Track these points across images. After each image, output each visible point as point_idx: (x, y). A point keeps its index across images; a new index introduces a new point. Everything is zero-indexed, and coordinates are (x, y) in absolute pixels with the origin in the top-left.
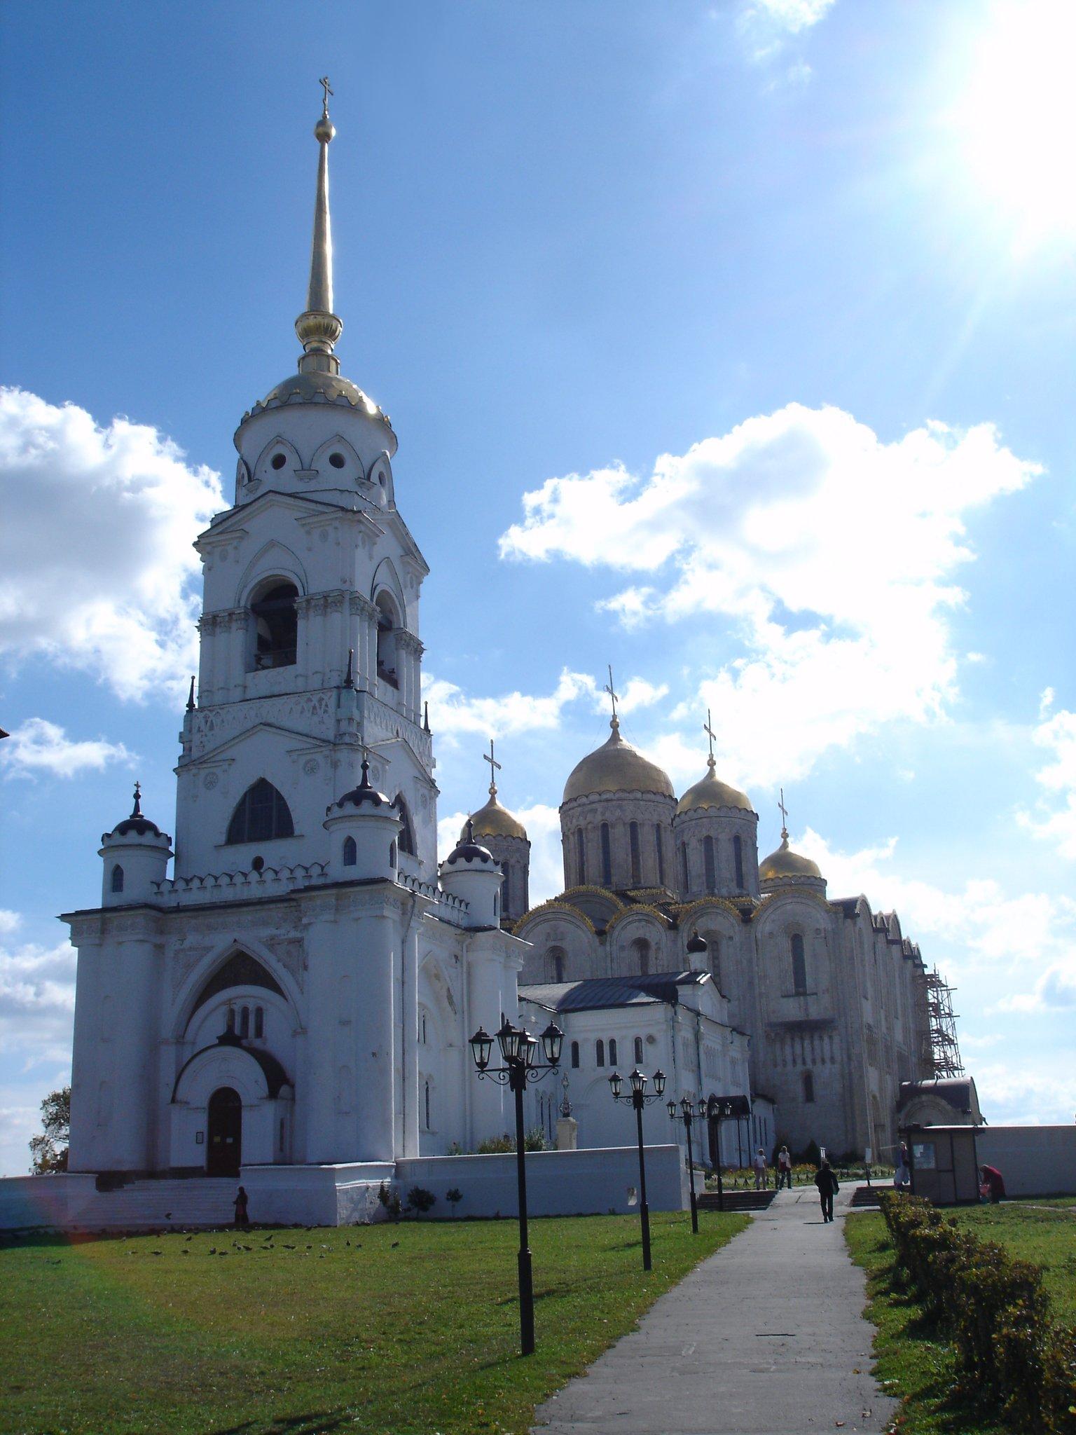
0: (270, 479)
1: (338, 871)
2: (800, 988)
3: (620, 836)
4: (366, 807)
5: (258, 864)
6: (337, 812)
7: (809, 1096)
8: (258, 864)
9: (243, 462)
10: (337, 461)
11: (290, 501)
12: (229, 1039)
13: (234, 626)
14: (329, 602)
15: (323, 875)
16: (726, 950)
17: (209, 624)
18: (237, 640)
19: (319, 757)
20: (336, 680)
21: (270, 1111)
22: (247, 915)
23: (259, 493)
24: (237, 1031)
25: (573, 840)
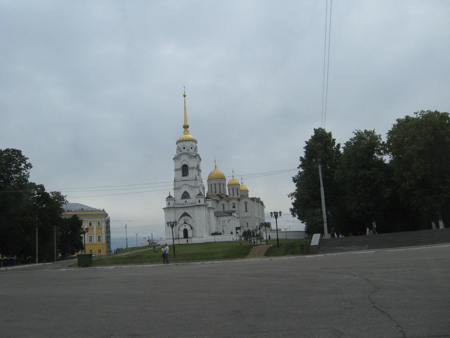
0: (183, 151)
1: (198, 204)
2: (246, 211)
3: (218, 186)
4: (201, 196)
5: (186, 201)
7: (248, 226)
8: (186, 201)
9: (178, 147)
10: (192, 148)
12: (185, 223)
14: (193, 168)
16: (236, 206)
17: (176, 170)
18: (180, 173)
21: (191, 231)
22: (186, 209)
25: (210, 186)
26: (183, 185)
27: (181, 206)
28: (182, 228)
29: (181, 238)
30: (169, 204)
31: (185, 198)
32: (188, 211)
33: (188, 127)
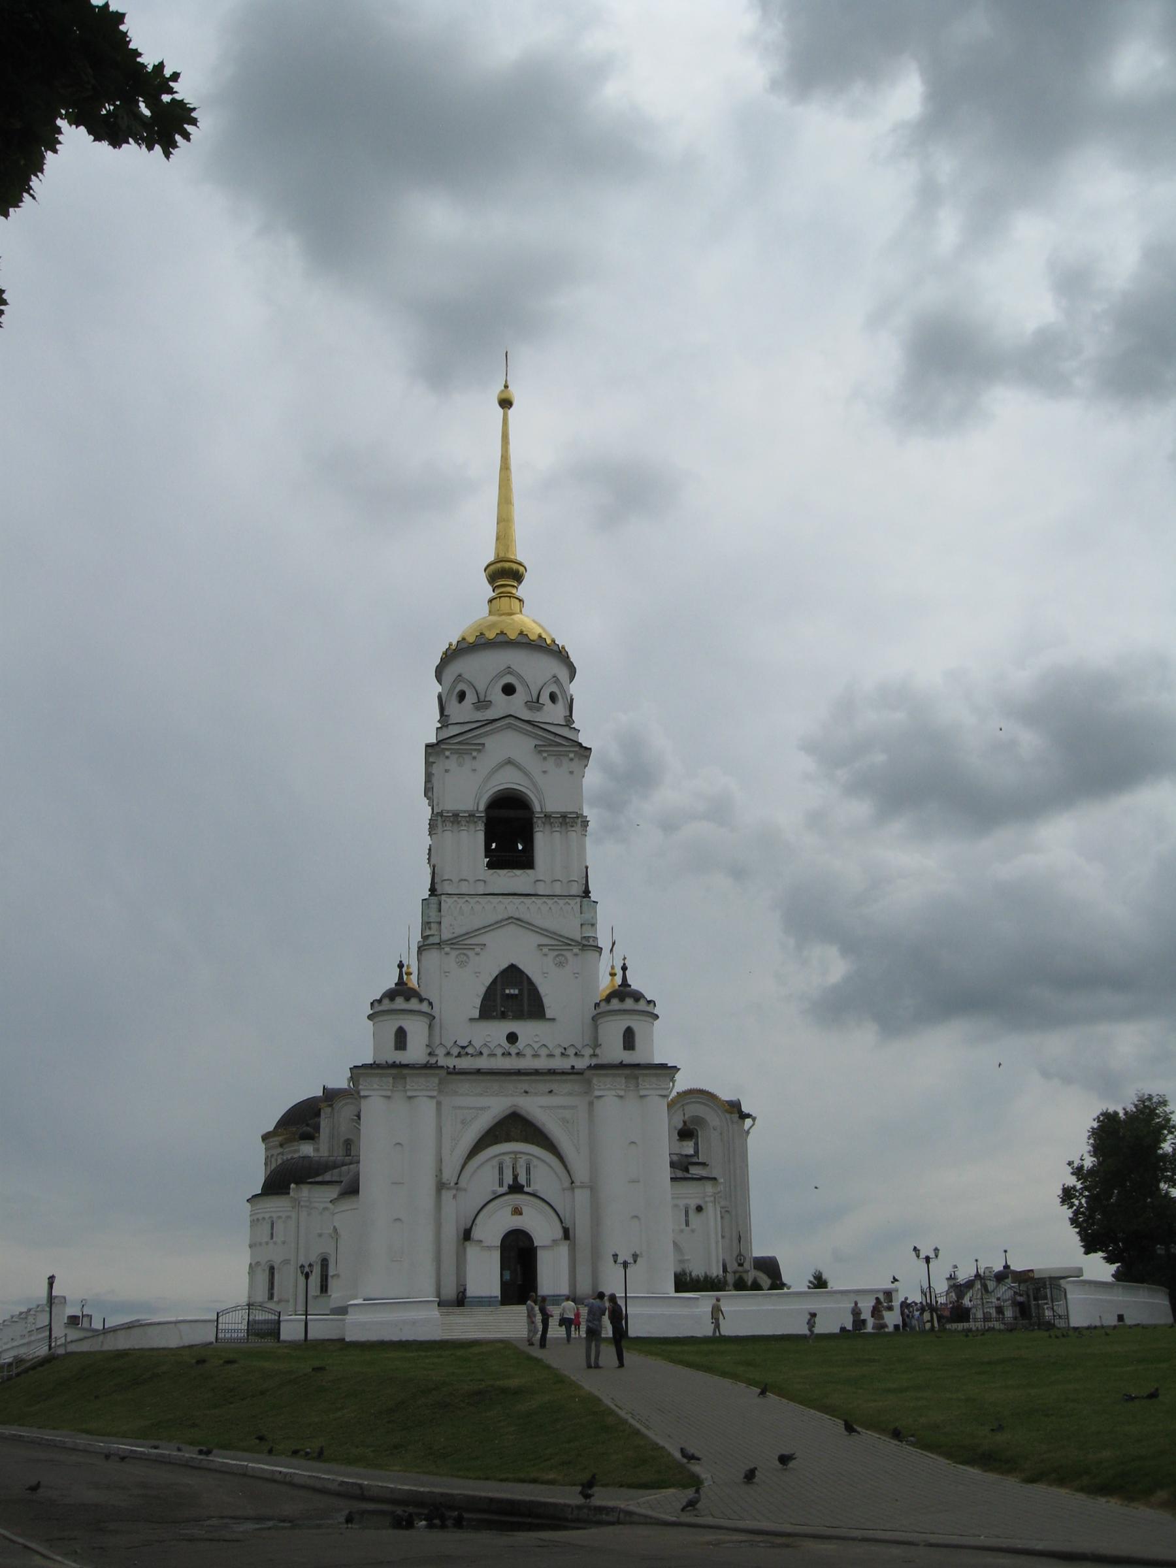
0: (501, 705)
5: (512, 1038)
6: (615, 1004)
8: (512, 1038)
10: (553, 698)
11: (529, 728)
12: (516, 1188)
13: (472, 827)
15: (594, 1055)
17: (441, 820)
18: (473, 840)
19: (568, 954)
20: (576, 889)
21: (564, 1249)
23: (490, 714)
24: (522, 1180)
26: (498, 924)
27: (483, 1063)
28: (495, 1226)
29: (483, 1302)
30: (401, 1040)
31: (503, 1016)
32: (537, 1106)
33: (518, 577)
